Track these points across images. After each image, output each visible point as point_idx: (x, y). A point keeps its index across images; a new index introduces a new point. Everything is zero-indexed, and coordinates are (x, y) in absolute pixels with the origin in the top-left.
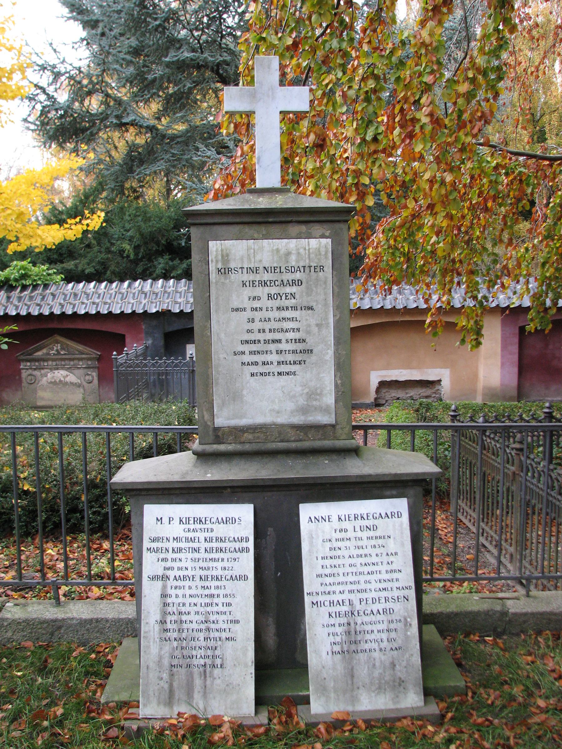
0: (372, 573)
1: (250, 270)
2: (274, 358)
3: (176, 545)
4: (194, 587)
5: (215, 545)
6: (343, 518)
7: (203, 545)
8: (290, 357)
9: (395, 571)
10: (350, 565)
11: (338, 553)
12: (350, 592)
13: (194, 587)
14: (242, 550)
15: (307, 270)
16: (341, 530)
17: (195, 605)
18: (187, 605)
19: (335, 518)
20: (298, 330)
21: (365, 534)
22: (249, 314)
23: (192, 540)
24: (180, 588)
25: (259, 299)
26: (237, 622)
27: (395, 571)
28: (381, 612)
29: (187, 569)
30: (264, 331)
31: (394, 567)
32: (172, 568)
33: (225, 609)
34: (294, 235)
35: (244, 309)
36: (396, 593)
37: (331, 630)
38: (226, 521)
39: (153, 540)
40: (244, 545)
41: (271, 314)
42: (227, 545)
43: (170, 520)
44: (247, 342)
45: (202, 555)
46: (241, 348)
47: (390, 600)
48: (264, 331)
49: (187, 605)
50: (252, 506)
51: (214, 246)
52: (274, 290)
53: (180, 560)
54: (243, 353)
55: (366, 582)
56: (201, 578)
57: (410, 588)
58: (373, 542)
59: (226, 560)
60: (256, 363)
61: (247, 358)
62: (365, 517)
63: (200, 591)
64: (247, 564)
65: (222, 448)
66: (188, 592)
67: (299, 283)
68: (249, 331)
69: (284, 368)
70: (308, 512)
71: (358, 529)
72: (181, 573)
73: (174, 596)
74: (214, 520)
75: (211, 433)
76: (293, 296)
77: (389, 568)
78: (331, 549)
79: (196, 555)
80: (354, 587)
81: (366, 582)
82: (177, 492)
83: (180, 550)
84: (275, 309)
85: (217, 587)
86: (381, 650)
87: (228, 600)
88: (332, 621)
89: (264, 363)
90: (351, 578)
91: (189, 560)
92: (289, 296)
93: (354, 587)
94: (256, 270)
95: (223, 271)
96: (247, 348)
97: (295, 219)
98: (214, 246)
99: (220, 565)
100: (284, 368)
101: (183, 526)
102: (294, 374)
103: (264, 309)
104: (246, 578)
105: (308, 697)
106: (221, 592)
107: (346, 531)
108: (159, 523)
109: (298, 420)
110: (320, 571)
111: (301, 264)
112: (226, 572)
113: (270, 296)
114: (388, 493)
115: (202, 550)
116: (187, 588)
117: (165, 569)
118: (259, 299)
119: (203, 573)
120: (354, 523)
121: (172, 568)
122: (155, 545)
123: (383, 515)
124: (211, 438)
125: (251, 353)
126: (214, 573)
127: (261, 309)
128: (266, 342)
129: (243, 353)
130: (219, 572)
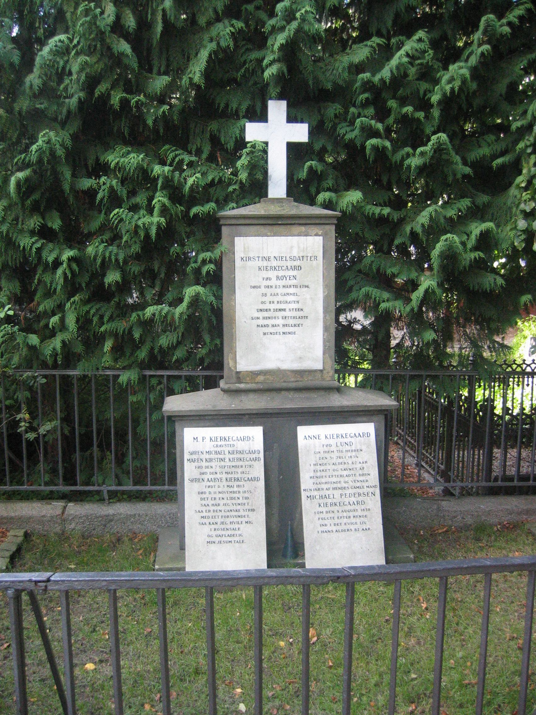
1: (264, 258)
2: (281, 322)
3: (208, 456)
4: (222, 486)
6: (328, 437)
7: (227, 456)
8: (292, 322)
10: (334, 470)
11: (325, 461)
13: (222, 486)
14: (255, 459)
15: (305, 259)
17: (223, 499)
18: (218, 499)
20: (298, 302)
22: (263, 290)
25: (270, 279)
26: (253, 510)
27: (365, 474)
30: (273, 302)
31: (365, 471)
33: (245, 501)
34: (296, 233)
35: (260, 287)
36: (366, 490)
37: (321, 516)
39: (192, 454)
41: (279, 291)
42: (245, 456)
44: (261, 310)
45: (228, 463)
46: (257, 315)
48: (273, 302)
49: (218, 499)
51: (239, 241)
52: (281, 273)
54: (258, 318)
58: (349, 454)
60: (267, 326)
61: (261, 322)
62: (344, 436)
63: (226, 489)
64: (259, 470)
65: (242, 386)
66: (217, 490)
67: (299, 268)
68: (263, 303)
69: (287, 329)
71: (339, 444)
72: (213, 476)
75: (234, 375)
76: (295, 277)
79: (222, 463)
80: (335, 485)
82: (210, 417)
83: (211, 460)
84: (281, 287)
85: (238, 486)
87: (246, 495)
88: (320, 509)
89: (273, 326)
90: (334, 479)
92: (292, 278)
94: (269, 259)
95: (245, 259)
96: (261, 315)
97: (297, 222)
98: (239, 241)
99: (240, 470)
100: (287, 329)
101: (213, 443)
102: (294, 333)
103: (274, 287)
105: (304, 563)
106: (241, 490)
107: (331, 446)
109: (296, 366)
111: (301, 255)
113: (278, 277)
114: (359, 419)
115: (227, 460)
116: (216, 487)
118: (270, 279)
119: (229, 476)
122: (194, 457)
123: (357, 435)
124: (234, 380)
125: (264, 318)
126: (236, 476)
127: (271, 287)
128: (276, 310)
129: (258, 318)
130: (239, 476)
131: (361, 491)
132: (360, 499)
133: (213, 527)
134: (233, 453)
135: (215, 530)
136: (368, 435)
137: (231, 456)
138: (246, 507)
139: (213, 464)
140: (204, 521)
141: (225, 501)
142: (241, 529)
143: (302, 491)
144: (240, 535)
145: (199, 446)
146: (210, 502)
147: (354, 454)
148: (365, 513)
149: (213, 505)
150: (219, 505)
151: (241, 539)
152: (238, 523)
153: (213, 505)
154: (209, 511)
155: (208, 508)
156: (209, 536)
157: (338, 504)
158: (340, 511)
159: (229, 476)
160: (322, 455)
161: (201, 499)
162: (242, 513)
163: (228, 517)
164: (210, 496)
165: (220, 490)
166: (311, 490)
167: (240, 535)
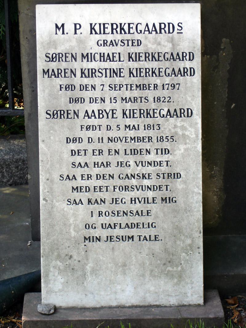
4: (114, 127)
13: (114, 127)
14: (184, 72)
18: (106, 153)
23: (110, 58)
24: (94, 128)
29: (103, 100)
32: (82, 100)
40: (188, 64)
45: (126, 80)
56: (124, 114)
59: (160, 87)
72: (96, 107)
74: (141, 28)
79: (117, 80)
83: (92, 73)
85: (148, 127)
91: (107, 88)
99: (150, 94)
104: (189, 114)
115: (126, 73)
116: (104, 128)
119: (129, 106)
121: (82, 100)
122: (53, 65)
126: (144, 106)
133: (96, 208)
135: (100, 214)
137: (134, 65)
138: (164, 169)
139: (97, 81)
140: (77, 196)
141: (121, 158)
142: (153, 212)
145: (66, 44)
150: (108, 164)
151: (152, 232)
154: (89, 177)
156: (87, 226)
159: (129, 106)
165: (111, 134)
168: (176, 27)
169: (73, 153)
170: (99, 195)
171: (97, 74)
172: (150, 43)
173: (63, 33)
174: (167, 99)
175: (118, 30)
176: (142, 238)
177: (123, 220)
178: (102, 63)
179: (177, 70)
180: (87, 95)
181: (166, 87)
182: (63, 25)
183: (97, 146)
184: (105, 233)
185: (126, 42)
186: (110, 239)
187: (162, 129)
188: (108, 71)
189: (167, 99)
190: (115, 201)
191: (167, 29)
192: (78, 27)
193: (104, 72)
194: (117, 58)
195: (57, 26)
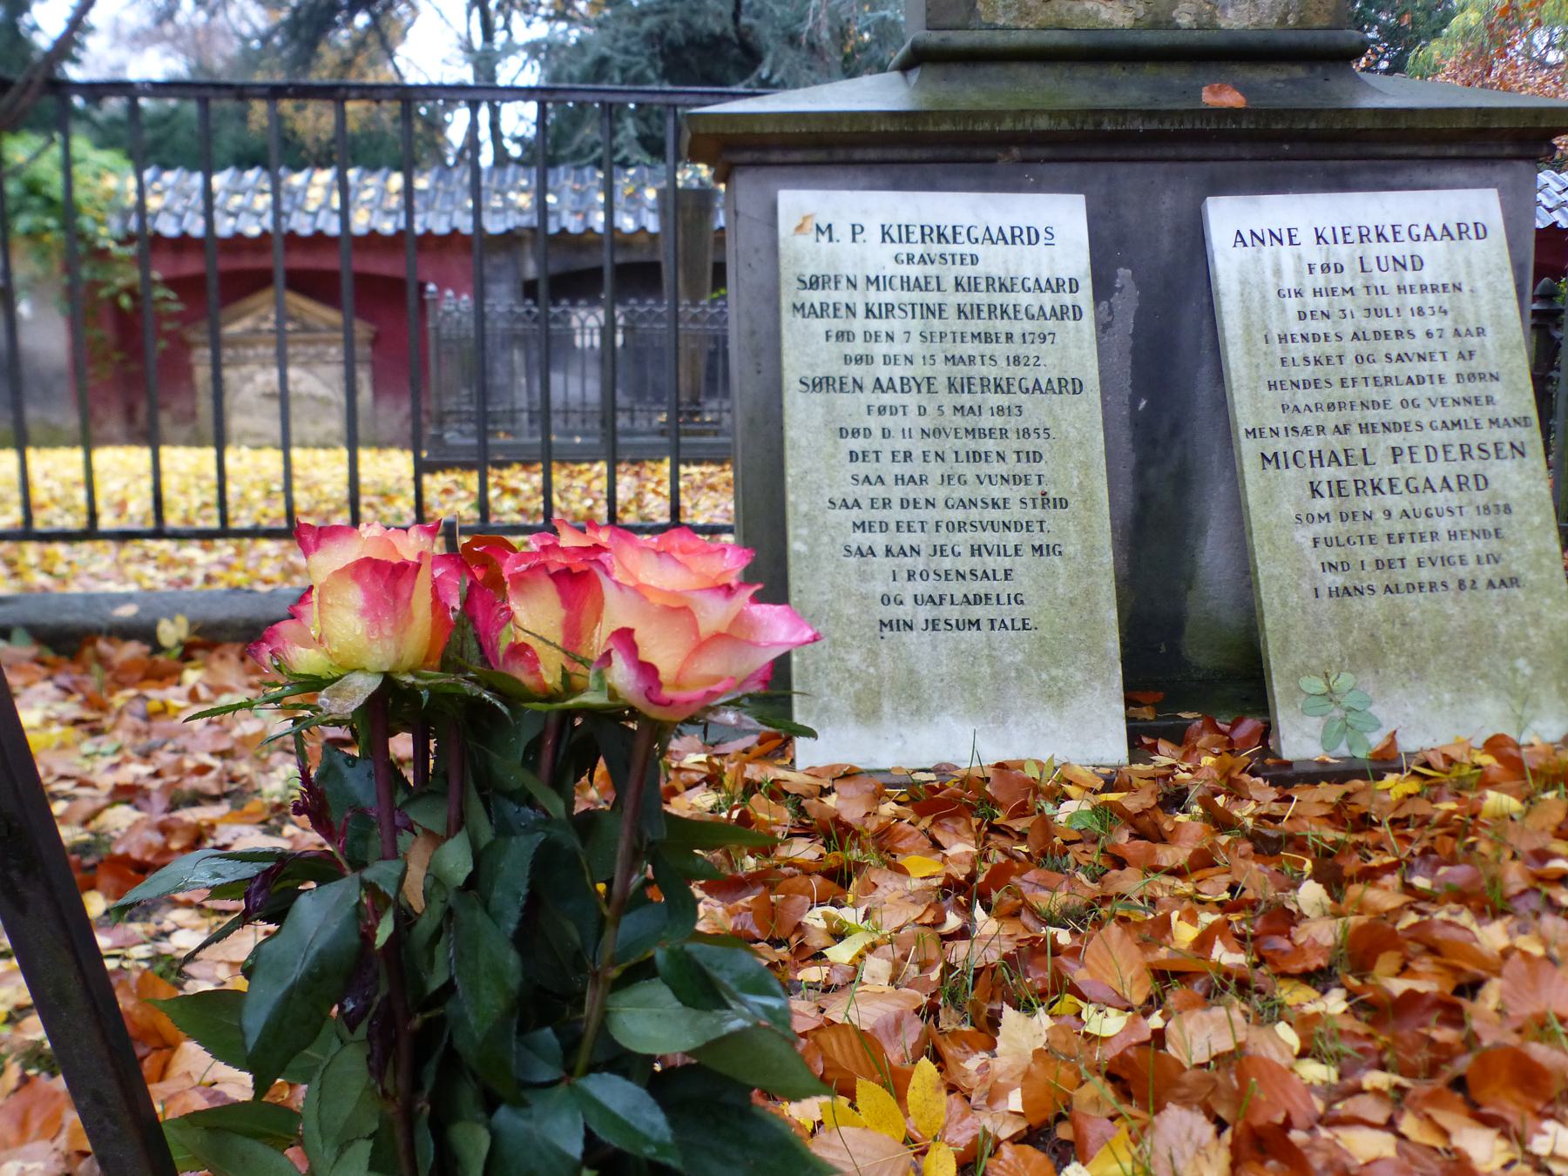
0: (1421, 380)
3: (876, 297)
5: (981, 298)
6: (1328, 235)
7: (953, 299)
9: (1482, 377)
10: (1359, 359)
12: (1364, 428)
14: (1060, 314)
16: (1325, 268)
19: (1305, 236)
21: (1390, 279)
24: (894, 411)
27: (1482, 377)
28: (1453, 483)
31: (1475, 365)
33: (1022, 468)
36: (1489, 435)
38: (1012, 237)
39: (815, 283)
42: (1024, 299)
43: (856, 231)
45: (954, 324)
47: (1476, 452)
50: (1080, 200)
53: (890, 337)
55: (1404, 403)
57: (1522, 422)
58: (1413, 300)
62: (1388, 233)
70: (1227, 217)
72: (898, 372)
73: (877, 433)
74: (978, 233)
77: (1463, 367)
78: (1302, 316)
79: (936, 324)
81: (1404, 403)
83: (889, 310)
86: (1461, 584)
87: (1029, 445)
91: (915, 336)
93: (1372, 416)
99: (1000, 349)
104: (1078, 386)
106: (1012, 423)
107: (1339, 269)
108: (824, 239)
110: (1279, 374)
112: (1021, 371)
115: (951, 312)
117: (847, 359)
119: (961, 371)
120: (1358, 249)
122: (816, 297)
123: (1437, 231)
126: (991, 372)
131: (1473, 437)
132: (1471, 466)
134: (973, 285)
135: (911, 576)
136: (1481, 232)
139: (895, 324)
143: (1242, 433)
144: (1017, 599)
146: (890, 469)
147: (1431, 299)
148: (1487, 522)
149: (899, 479)
151: (1017, 612)
152: (1002, 551)
153: (899, 479)
154: (886, 503)
155: (878, 491)
156: (886, 600)
157: (1385, 487)
158: (1396, 513)
159: (961, 371)
160: (1312, 303)
161: (853, 456)
162: (1015, 513)
163: (961, 526)
164: (887, 447)
166: (1275, 432)
167: (1017, 599)
168: (1042, 234)
169: (853, 456)
170: (906, 539)
171: (897, 312)
172: (994, 260)
173: (831, 239)
174: (1032, 361)
175: (935, 236)
176: (997, 625)
177: (957, 588)
178: (905, 293)
179: (1048, 311)
180: (880, 349)
181: (1029, 339)
182: (830, 226)
183: (902, 445)
184: (926, 612)
185: (949, 258)
186: (933, 624)
187: (1025, 413)
188: (918, 309)
189: (1032, 361)
190: (939, 551)
191: (1025, 237)
192: (858, 229)
193: (909, 309)
194: (934, 284)
195: (818, 228)
